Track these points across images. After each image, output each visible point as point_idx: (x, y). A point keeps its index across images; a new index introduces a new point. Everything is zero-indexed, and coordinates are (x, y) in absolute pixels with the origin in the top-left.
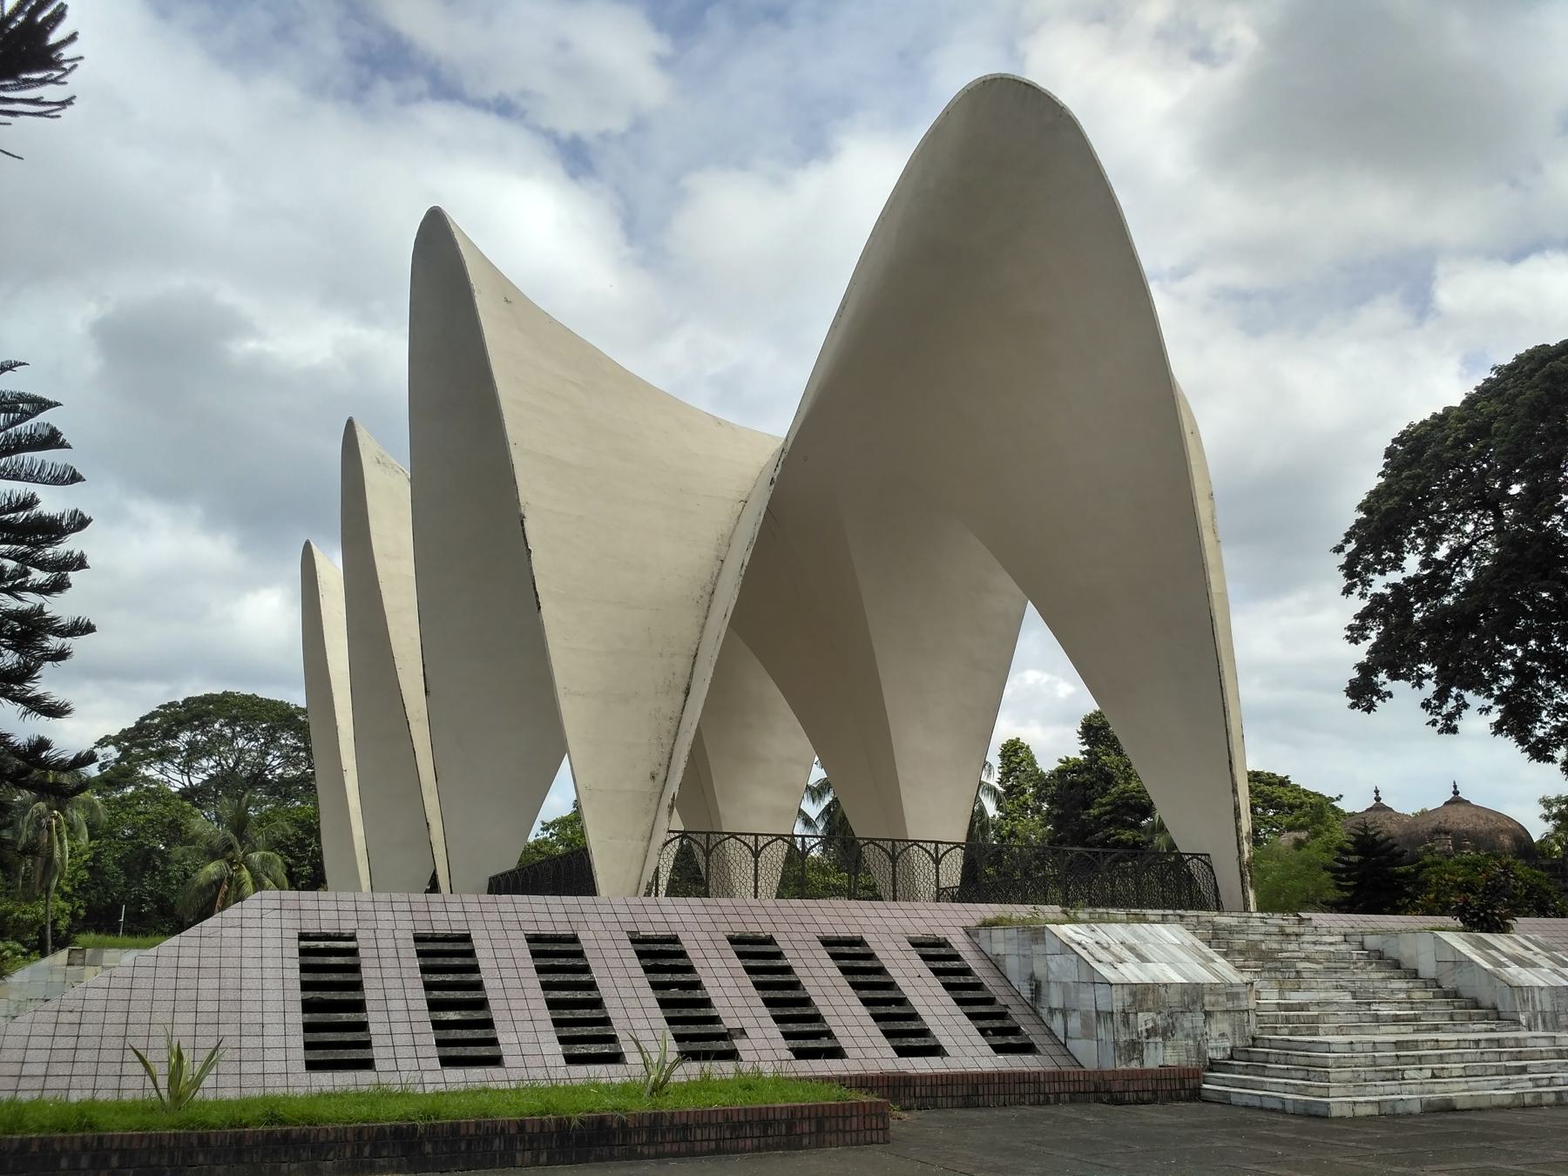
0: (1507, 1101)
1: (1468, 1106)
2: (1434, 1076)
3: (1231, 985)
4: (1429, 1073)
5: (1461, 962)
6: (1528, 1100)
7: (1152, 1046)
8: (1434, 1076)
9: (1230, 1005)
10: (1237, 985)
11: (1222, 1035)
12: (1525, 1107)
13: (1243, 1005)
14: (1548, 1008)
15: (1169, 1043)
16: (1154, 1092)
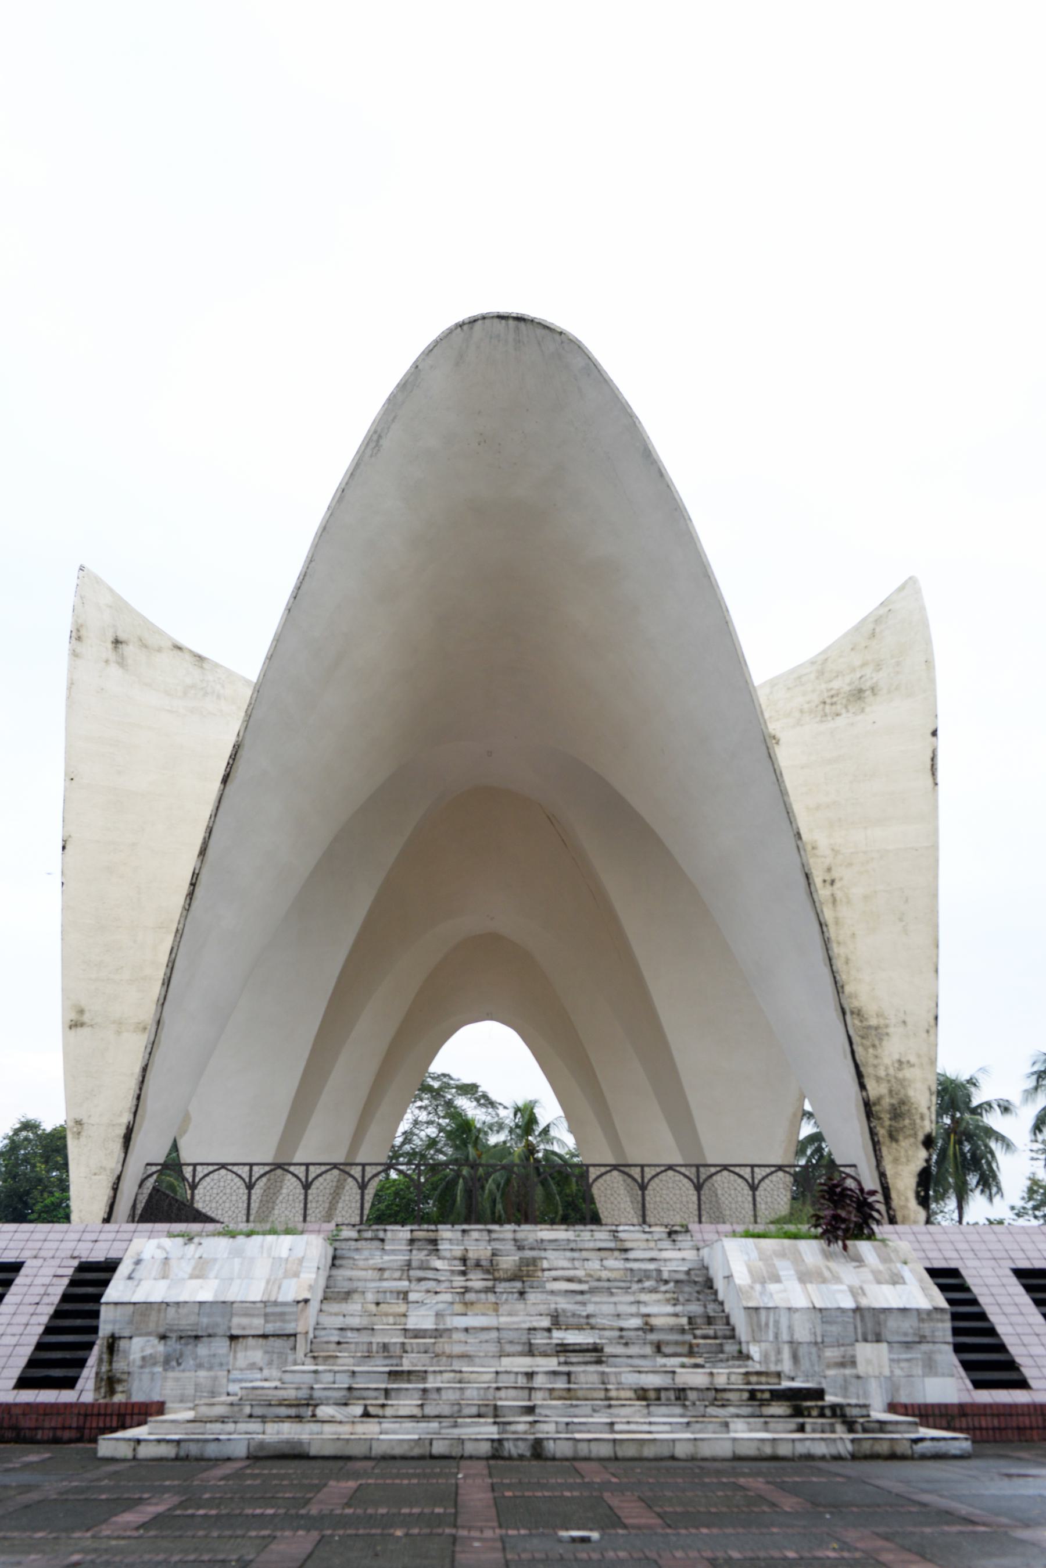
0: (398, 1451)
1: (328, 1451)
2: (366, 1415)
3: (276, 1303)
4: (359, 1410)
5: (729, 1277)
6: (438, 1448)
7: (146, 1377)
8: (366, 1415)
9: (270, 1328)
10: (285, 1304)
11: (252, 1366)
12: (432, 1457)
13: (290, 1328)
14: (803, 1335)
15: (170, 1374)
16: (80, 1429)
